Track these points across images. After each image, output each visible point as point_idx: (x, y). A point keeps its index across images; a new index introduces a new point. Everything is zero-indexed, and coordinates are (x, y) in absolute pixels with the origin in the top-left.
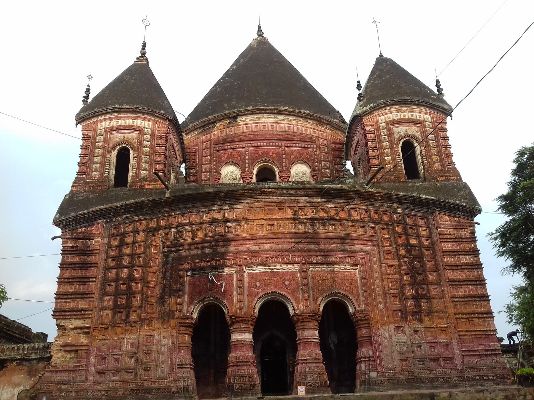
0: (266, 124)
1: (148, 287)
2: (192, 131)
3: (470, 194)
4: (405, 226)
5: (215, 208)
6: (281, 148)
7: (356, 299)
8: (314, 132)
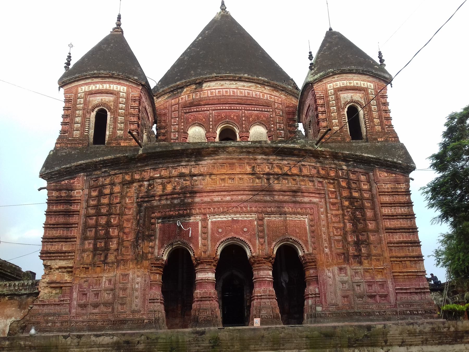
0: (228, 90)
1: (124, 233)
2: (162, 95)
3: (406, 153)
4: (348, 180)
5: (183, 164)
6: (241, 111)
7: (305, 244)
8: (271, 98)
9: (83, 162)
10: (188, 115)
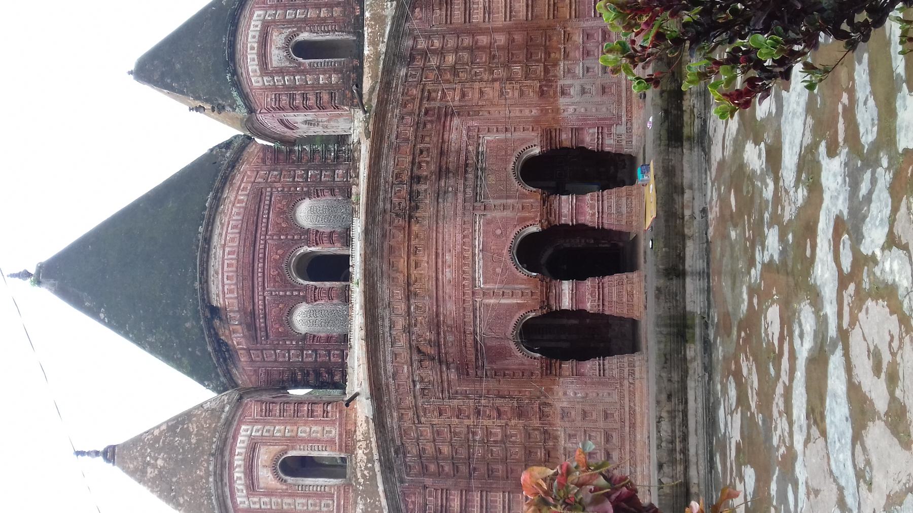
0: (226, 262)
8: (245, 189)
9: (381, 488)
10: (270, 334)
